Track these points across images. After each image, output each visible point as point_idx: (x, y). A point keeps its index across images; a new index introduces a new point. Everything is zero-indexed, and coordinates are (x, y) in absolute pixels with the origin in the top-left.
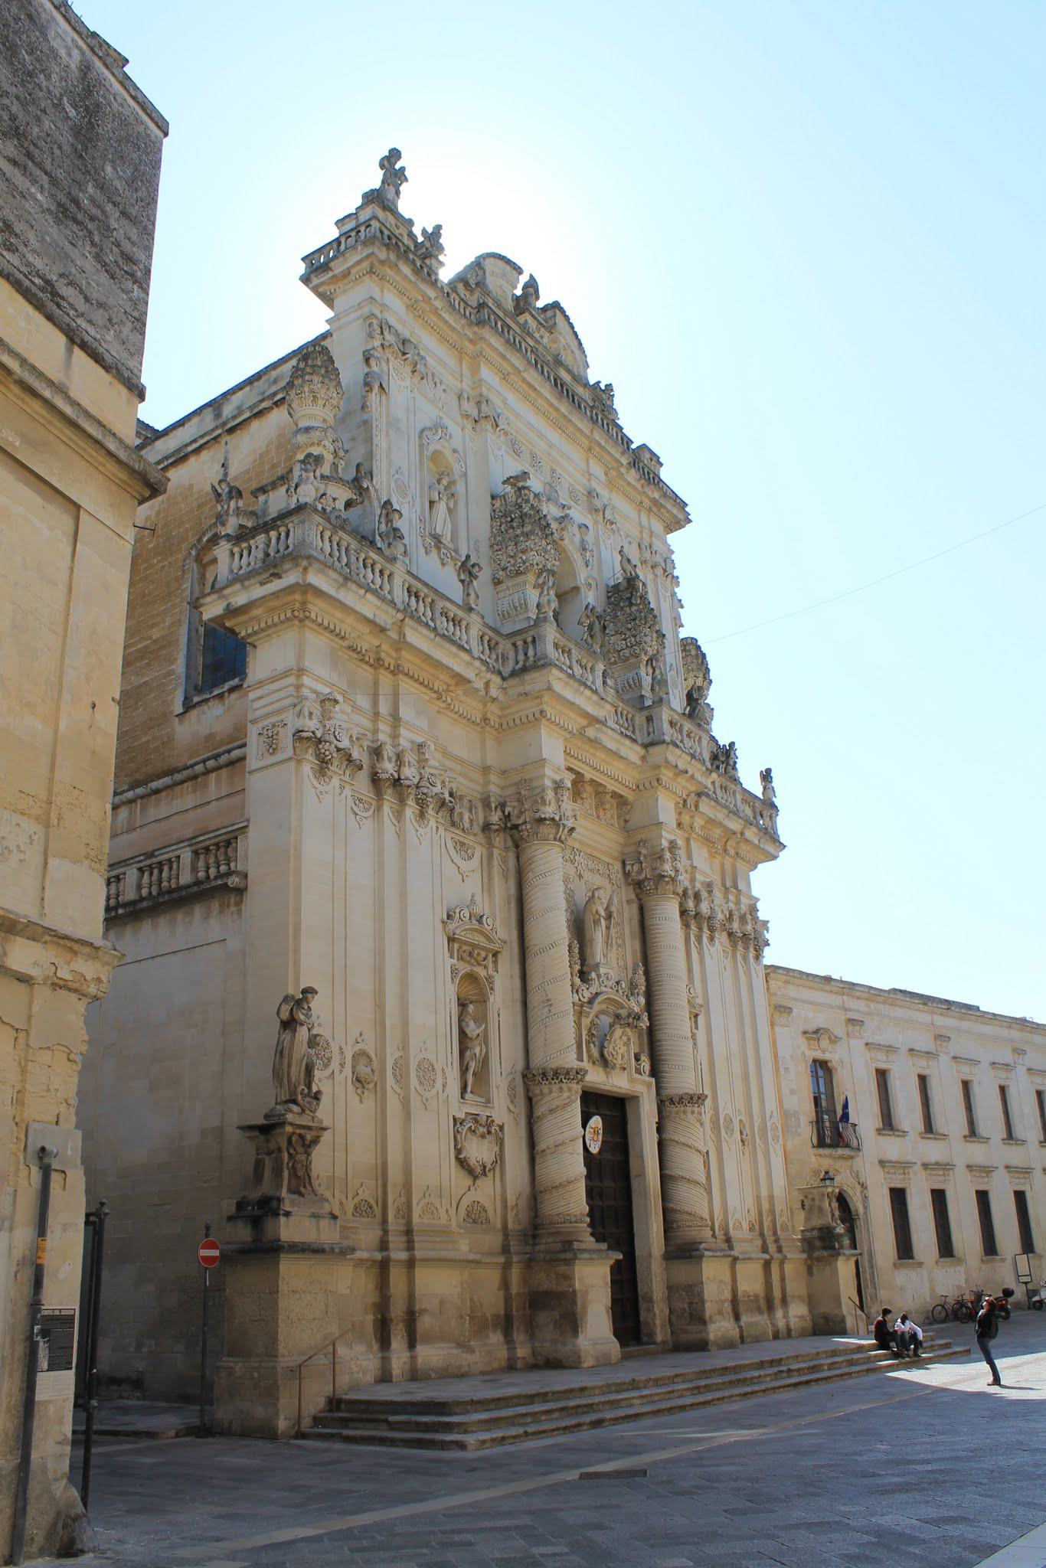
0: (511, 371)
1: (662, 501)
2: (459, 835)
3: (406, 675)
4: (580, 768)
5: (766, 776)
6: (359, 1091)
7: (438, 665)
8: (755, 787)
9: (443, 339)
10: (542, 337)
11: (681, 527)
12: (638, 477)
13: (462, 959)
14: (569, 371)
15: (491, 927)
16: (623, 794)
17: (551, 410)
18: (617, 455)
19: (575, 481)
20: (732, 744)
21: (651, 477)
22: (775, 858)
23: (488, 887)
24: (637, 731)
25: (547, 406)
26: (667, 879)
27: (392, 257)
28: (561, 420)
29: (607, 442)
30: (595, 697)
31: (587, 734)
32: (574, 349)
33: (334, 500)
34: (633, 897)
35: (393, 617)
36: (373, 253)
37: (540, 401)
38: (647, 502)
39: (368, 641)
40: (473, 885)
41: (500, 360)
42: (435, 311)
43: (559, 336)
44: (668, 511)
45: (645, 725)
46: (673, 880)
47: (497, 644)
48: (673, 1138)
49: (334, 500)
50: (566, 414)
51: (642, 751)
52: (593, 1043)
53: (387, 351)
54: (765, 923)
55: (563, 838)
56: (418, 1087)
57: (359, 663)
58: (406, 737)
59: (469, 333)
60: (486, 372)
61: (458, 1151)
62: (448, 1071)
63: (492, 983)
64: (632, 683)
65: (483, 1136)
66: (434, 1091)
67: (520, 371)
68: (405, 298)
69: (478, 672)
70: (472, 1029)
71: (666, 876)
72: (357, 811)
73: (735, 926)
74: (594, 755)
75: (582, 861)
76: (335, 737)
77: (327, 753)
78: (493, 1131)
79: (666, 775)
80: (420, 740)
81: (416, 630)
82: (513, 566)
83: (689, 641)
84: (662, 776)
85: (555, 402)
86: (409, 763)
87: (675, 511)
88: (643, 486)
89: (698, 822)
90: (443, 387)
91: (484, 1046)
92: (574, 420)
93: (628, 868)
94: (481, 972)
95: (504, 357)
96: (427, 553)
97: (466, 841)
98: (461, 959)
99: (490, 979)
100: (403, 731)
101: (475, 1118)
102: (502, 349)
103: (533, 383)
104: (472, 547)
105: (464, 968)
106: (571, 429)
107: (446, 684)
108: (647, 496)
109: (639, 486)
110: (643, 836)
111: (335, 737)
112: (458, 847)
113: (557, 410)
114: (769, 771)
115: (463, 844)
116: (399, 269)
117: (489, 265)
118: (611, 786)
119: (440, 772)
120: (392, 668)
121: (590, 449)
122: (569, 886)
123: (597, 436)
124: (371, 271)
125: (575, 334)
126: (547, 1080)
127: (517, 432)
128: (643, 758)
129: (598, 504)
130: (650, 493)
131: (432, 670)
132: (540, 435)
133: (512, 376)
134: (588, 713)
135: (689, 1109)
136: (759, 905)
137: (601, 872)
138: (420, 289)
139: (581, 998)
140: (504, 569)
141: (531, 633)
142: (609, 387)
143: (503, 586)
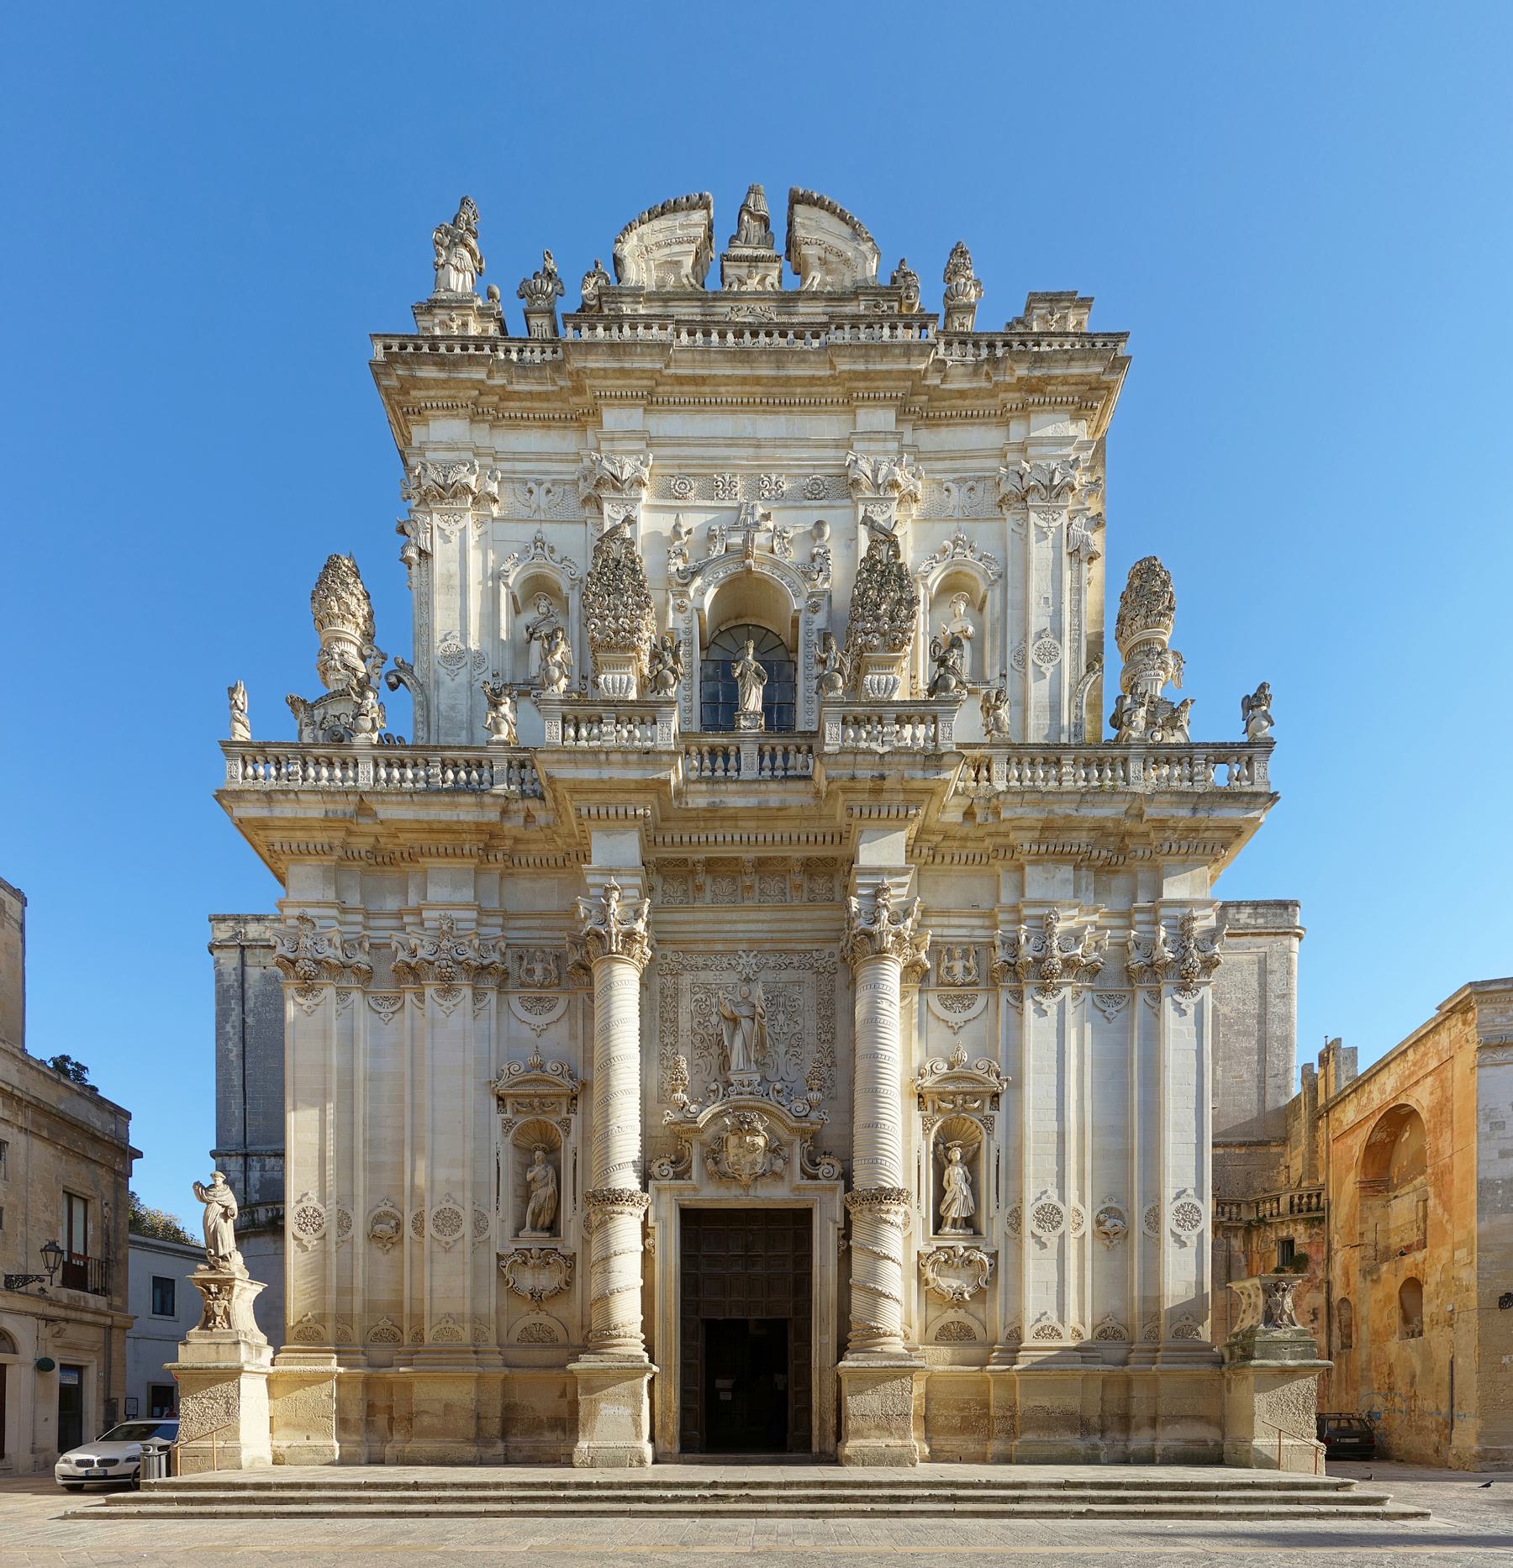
42: (506, 396)
44: (1065, 381)
56: (435, 1234)
57: (378, 868)
68: (460, 410)
75: (754, 961)
88: (988, 377)
97: (543, 995)
99: (566, 1124)
108: (1009, 388)
115: (539, 999)
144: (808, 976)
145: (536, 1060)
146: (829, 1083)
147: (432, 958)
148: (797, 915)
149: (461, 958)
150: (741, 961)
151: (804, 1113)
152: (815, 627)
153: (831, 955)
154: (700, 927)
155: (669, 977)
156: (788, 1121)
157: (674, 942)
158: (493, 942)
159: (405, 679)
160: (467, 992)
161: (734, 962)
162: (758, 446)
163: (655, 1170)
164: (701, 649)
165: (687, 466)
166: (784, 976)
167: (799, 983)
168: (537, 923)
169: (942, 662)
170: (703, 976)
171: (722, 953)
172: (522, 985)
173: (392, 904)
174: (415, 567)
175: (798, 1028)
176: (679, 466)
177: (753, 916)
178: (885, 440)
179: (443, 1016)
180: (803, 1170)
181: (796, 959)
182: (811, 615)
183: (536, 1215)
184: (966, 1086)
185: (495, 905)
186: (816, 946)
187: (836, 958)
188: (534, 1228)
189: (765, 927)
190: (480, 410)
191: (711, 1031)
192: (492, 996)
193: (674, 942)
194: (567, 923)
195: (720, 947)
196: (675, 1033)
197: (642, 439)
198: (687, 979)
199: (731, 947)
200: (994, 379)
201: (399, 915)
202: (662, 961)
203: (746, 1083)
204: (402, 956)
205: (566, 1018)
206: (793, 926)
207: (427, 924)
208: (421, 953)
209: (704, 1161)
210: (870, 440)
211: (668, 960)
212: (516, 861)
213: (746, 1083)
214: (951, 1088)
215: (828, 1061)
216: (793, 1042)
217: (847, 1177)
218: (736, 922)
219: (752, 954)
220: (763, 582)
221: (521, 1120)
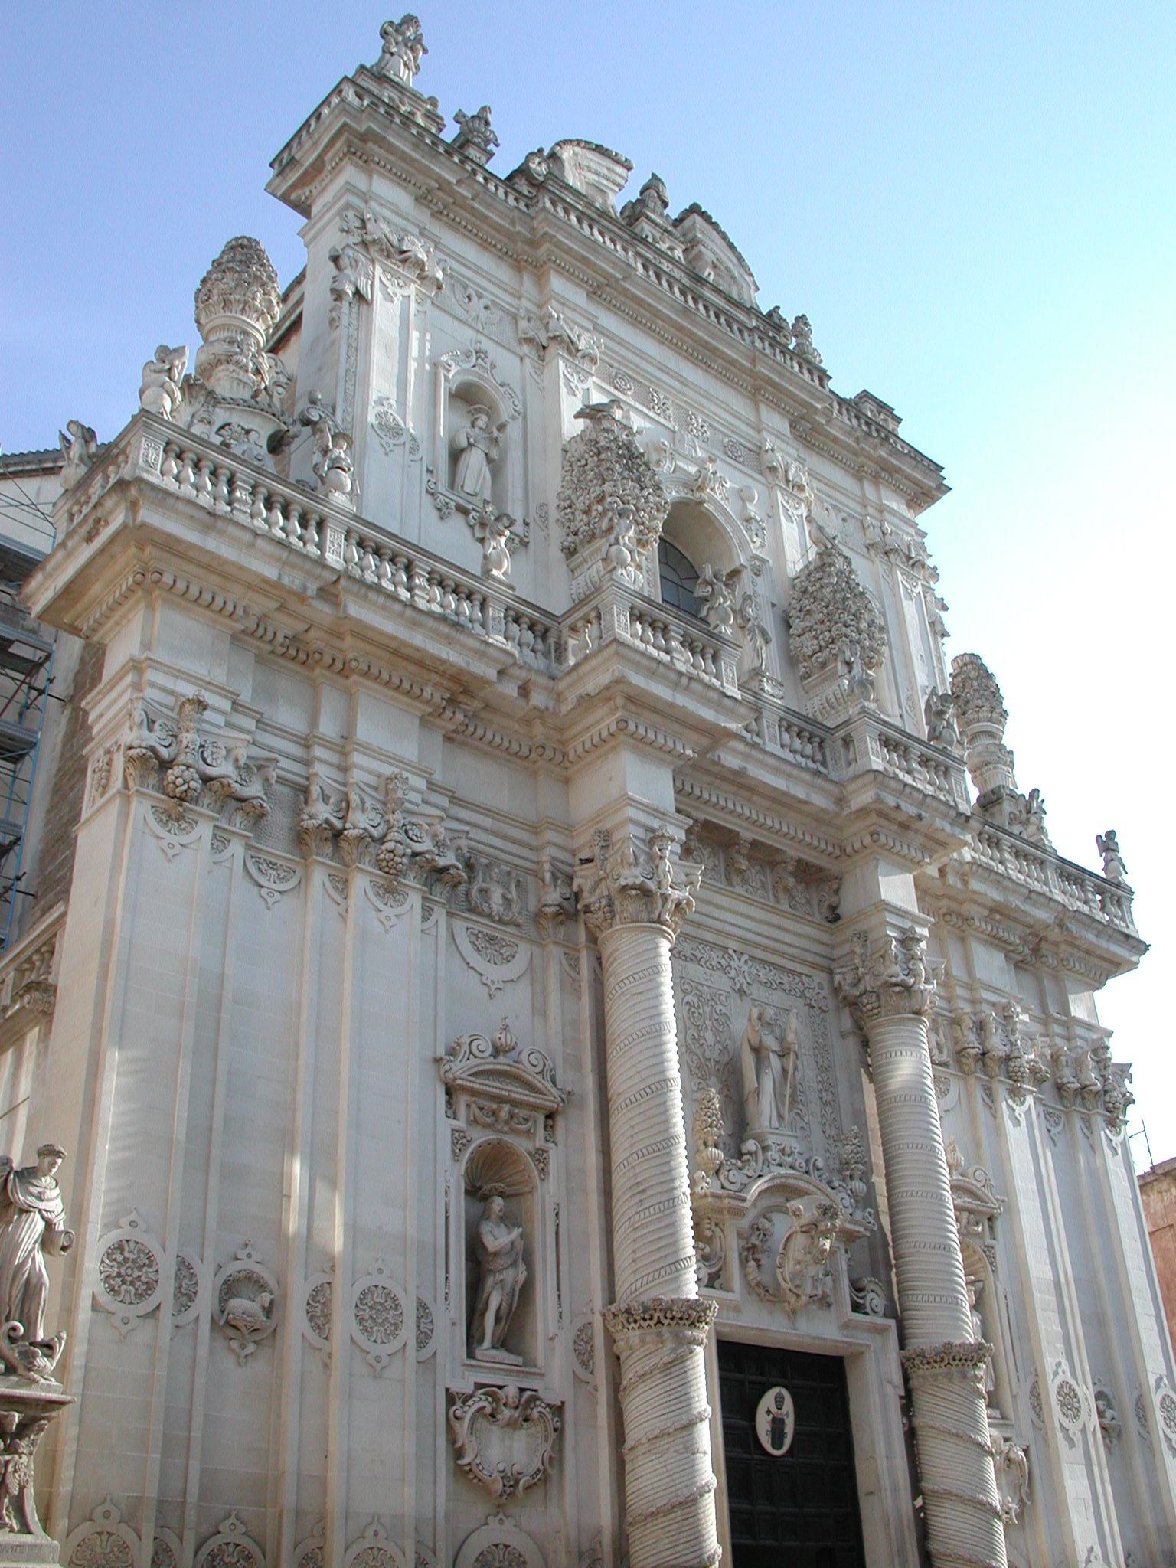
0: (602, 280)
2: (484, 926)
3: (366, 674)
5: (1107, 844)
6: (234, 1344)
8: (1095, 864)
9: (485, 245)
10: (671, 249)
11: (933, 500)
13: (476, 1121)
14: (716, 290)
15: (538, 1069)
20: (1035, 793)
21: (887, 436)
22: (1133, 965)
23: (540, 1011)
24: (830, 763)
26: (897, 989)
32: (730, 266)
33: (248, 432)
34: (847, 1023)
36: (345, 125)
37: (660, 323)
40: (517, 1002)
43: (702, 248)
44: (908, 477)
45: (842, 750)
47: (547, 630)
48: (931, 1423)
49: (248, 432)
52: (757, 1261)
53: (372, 249)
54: (1124, 1070)
58: (365, 769)
60: (557, 284)
61: (459, 1453)
62: (439, 1313)
63: (546, 1162)
64: (833, 700)
65: (512, 1424)
66: (395, 1344)
69: (499, 667)
70: (496, 1238)
71: (896, 985)
72: (262, 880)
73: (1067, 1075)
74: (749, 800)
75: (745, 968)
76: (204, 760)
77: (179, 781)
78: (535, 1414)
80: (388, 770)
82: (588, 524)
83: (967, 659)
86: (363, 802)
90: (485, 301)
91: (522, 1267)
93: (838, 978)
94: (522, 1145)
96: (442, 518)
98: (474, 1122)
99: (540, 1157)
100: (357, 758)
101: (492, 1392)
104: (533, 511)
105: (480, 1137)
110: (860, 927)
111: (204, 760)
112: (481, 943)
114: (1111, 834)
115: (491, 939)
117: (566, 154)
122: (719, 1007)
124: (350, 153)
125: (731, 246)
126: (635, 1322)
136: (1111, 1042)
137: (786, 987)
139: (726, 1184)
140: (576, 534)
141: (592, 604)
142: (801, 319)
143: (578, 559)
161: (723, 962)
165: (626, 366)
168: (487, 822)
174: (345, 304)
179: (379, 928)
181: (785, 980)
186: (805, 970)
190: (429, 198)
191: (708, 1055)
195: (709, 936)
199: (720, 940)
213: (787, 1150)
219: (743, 959)
220: (707, 519)
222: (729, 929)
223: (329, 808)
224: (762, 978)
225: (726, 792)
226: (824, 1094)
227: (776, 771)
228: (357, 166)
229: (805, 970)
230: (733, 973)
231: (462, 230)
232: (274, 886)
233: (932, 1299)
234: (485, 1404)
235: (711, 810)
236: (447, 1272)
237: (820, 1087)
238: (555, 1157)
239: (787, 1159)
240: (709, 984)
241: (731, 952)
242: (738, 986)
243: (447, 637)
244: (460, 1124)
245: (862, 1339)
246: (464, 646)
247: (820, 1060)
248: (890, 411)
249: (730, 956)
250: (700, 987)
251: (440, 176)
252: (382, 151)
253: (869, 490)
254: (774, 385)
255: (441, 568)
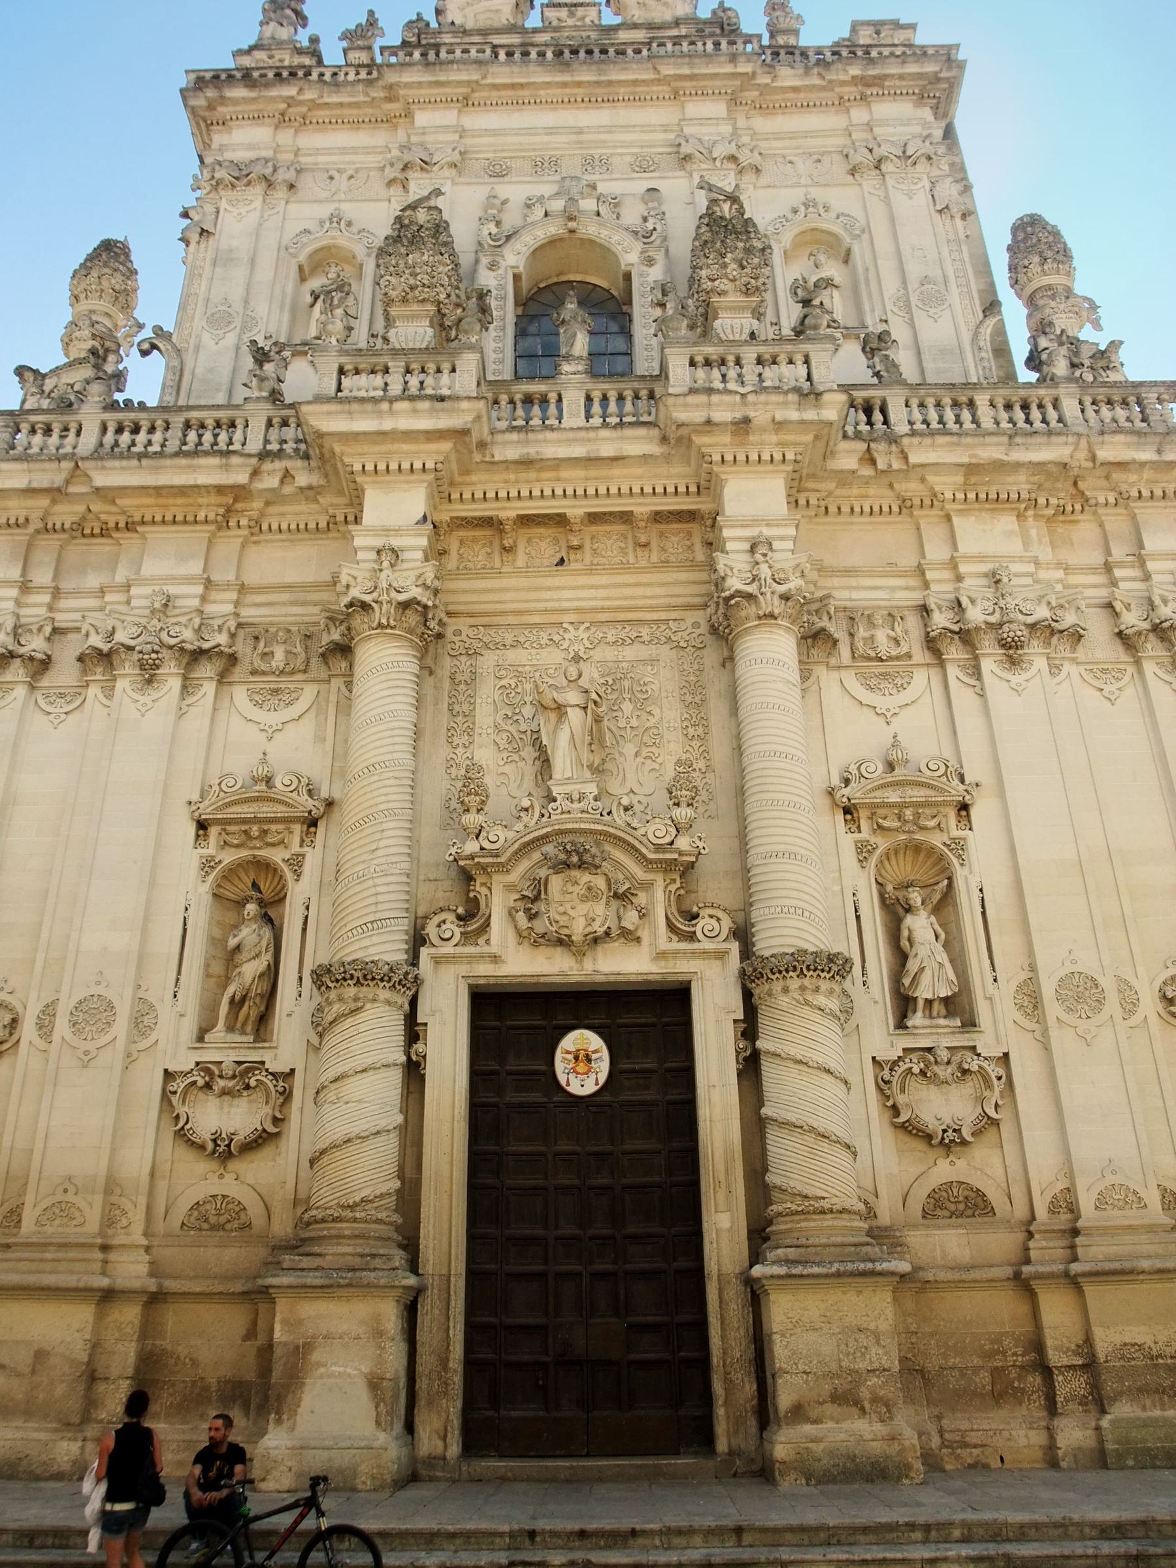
1: (872, 72)
3: (143, 523)
4: (555, 507)
7: (182, 491)
9: (356, 124)
10: (583, 18)
12: (801, 71)
14: (635, 26)
16: (685, 507)
17: (568, 91)
18: (729, 69)
19: (642, 147)
25: (560, 91)
26: (733, 602)
27: (211, 93)
28: (598, 91)
29: (691, 65)
30: (425, 405)
31: (497, 458)
35: (60, 470)
37: (542, 92)
38: (850, 91)
39: (67, 514)
41: (436, 91)
42: (314, 105)
44: (901, 77)
46: (750, 597)
50: (594, 78)
51: (655, 432)
55: (384, 621)
57: (84, 541)
59: (378, 93)
67: (477, 82)
71: (732, 597)
72: (49, 709)
75: (585, 636)
78: (253, 1083)
79: (717, 445)
81: (103, 468)
84: (704, 450)
85: (566, 78)
87: (912, 68)
88: (823, 78)
89: (947, 485)
92: (614, 76)
94: (277, 856)
95: (438, 84)
97: (282, 686)
102: (427, 77)
103: (509, 81)
106: (622, 90)
107: (220, 505)
108: (843, 83)
109: (817, 81)
113: (579, 84)
115: (276, 692)
116: (230, 99)
118: (642, 508)
119: (188, 617)
120: (122, 525)
121: (676, 94)
123: (668, 70)
127: (495, 151)
128: (664, 439)
129: (685, 149)
130: (842, 77)
131: (180, 501)
132: (551, 131)
133: (476, 95)
134: (427, 432)
135: (777, 986)
137: (646, 638)
138: (271, 98)
144: (665, 652)
145: (262, 771)
146: (703, 795)
147: (132, 643)
148: (644, 578)
149: (172, 642)
150: (567, 636)
151: (668, 839)
152: (651, 279)
153: (696, 625)
154: (509, 596)
155: (463, 659)
156: (644, 850)
157: (471, 615)
158: (220, 622)
159: (161, 345)
160: (175, 684)
161: (556, 638)
162: (580, 133)
163: (431, 930)
164: (517, 304)
166: (630, 653)
167: (653, 661)
168: (285, 597)
169: (806, 303)
170: (512, 656)
171: (539, 626)
172: (254, 672)
173: (93, 581)
175: (653, 721)
176: (495, 151)
177: (582, 580)
178: (717, 125)
180: (671, 926)
181: (645, 632)
182: (645, 268)
183: (237, 1004)
184: (918, 794)
185: (231, 577)
186: (674, 615)
187: (704, 628)
188: (230, 1028)
189: (601, 593)
191: (523, 727)
192: (209, 688)
193: (471, 615)
194: (325, 596)
195: (536, 619)
196: (470, 731)
197: (456, 132)
198: (489, 660)
200: (828, 77)
201: (102, 591)
202: (456, 639)
203: (576, 796)
204: (96, 641)
205: (311, 715)
206: (640, 591)
207: (134, 603)
208: (121, 637)
209: (511, 913)
210: (702, 124)
211: (464, 637)
212: (265, 527)
213: (576, 796)
214: (893, 797)
215: (701, 764)
216: (646, 739)
217: (743, 934)
218: (558, 588)
219: (583, 627)
221: (229, 857)
222: (565, 605)
223: (99, 637)
224: (611, 638)
225: (529, 482)
226: (691, 731)
227: (570, 442)
228: (220, 132)
229: (674, 615)
230: (565, 645)
231: (330, 127)
232: (58, 710)
233: (785, 910)
234: (198, 1078)
235: (519, 504)
236: (179, 973)
237: (685, 723)
238: (312, 859)
239: (576, 805)
240: (535, 662)
241: (565, 625)
242: (572, 654)
243: (190, 467)
244: (211, 851)
245: (680, 968)
246: (207, 467)
247: (689, 698)
248: (896, 25)
249: (566, 630)
250: (520, 669)
251: (281, 97)
252: (230, 109)
253: (859, 115)
254: (692, 77)
255: (194, 415)
